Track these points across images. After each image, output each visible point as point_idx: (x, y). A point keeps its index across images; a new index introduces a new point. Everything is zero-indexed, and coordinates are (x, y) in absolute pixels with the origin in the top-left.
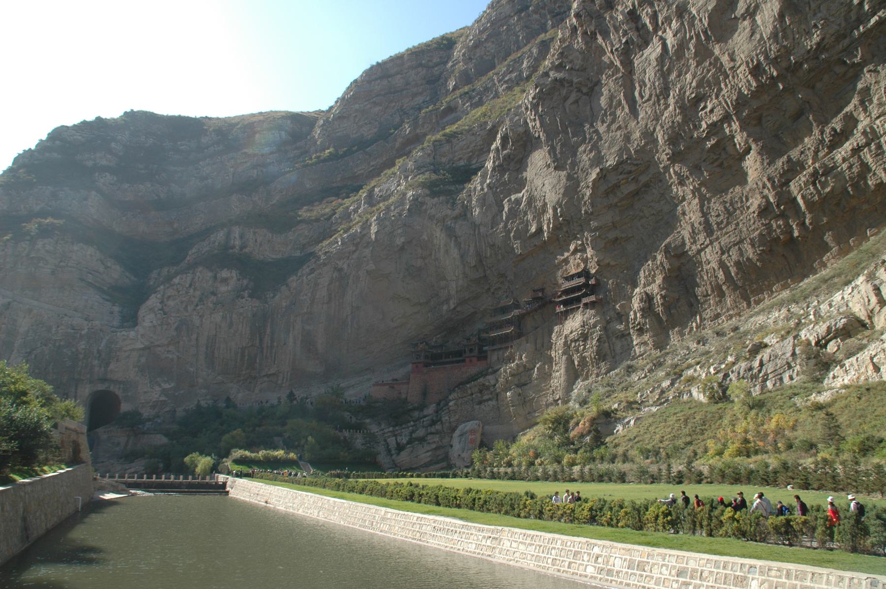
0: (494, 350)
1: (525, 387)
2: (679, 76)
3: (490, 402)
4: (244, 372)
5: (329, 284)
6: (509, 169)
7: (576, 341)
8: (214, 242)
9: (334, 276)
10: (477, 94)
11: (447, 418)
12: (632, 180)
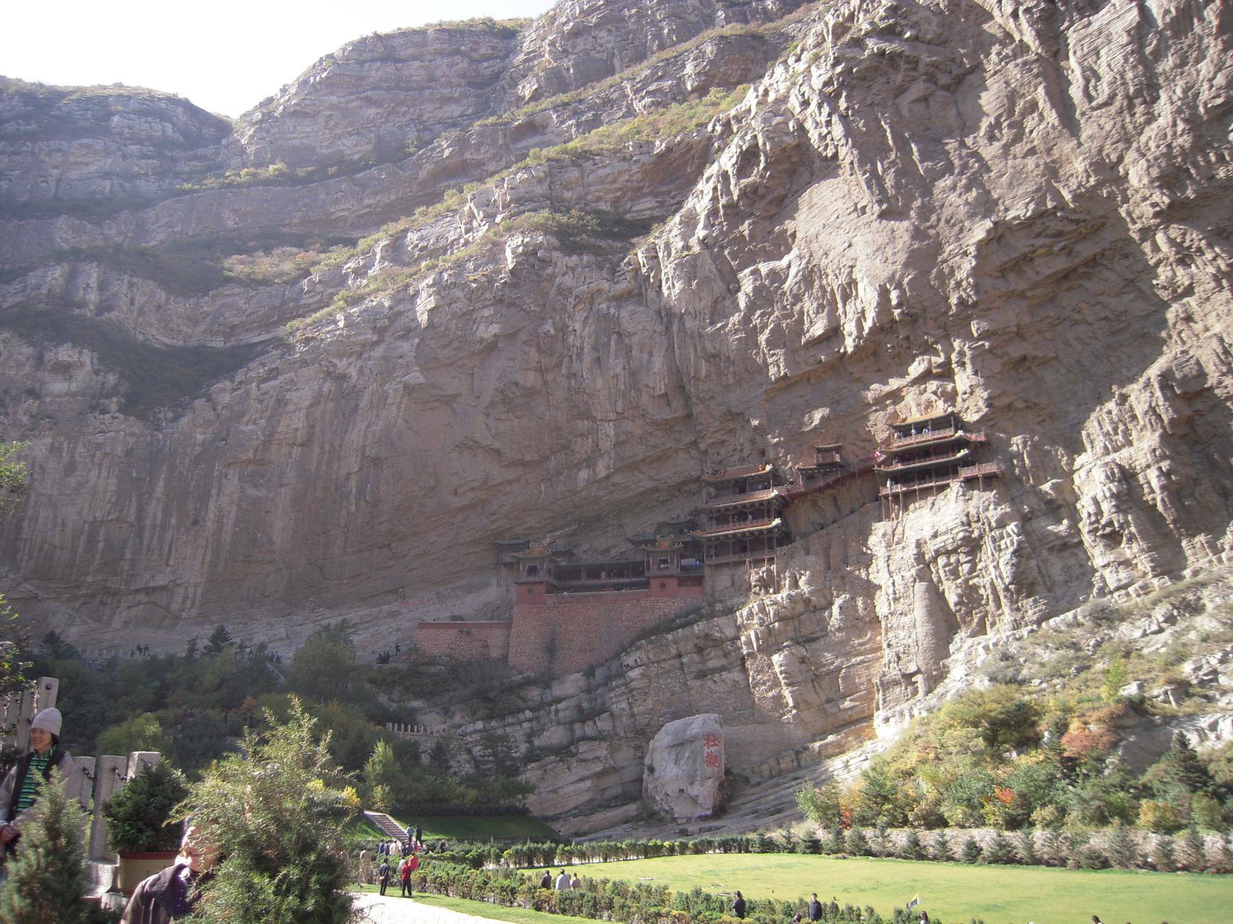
0: (718, 566)
1: (814, 645)
2: (1183, 63)
3: (725, 675)
4: (90, 579)
5: (312, 406)
6: (749, 216)
7: (948, 553)
8: (39, 287)
9: (325, 389)
10: (590, 109)
11: (624, 705)
12: (1062, 249)
